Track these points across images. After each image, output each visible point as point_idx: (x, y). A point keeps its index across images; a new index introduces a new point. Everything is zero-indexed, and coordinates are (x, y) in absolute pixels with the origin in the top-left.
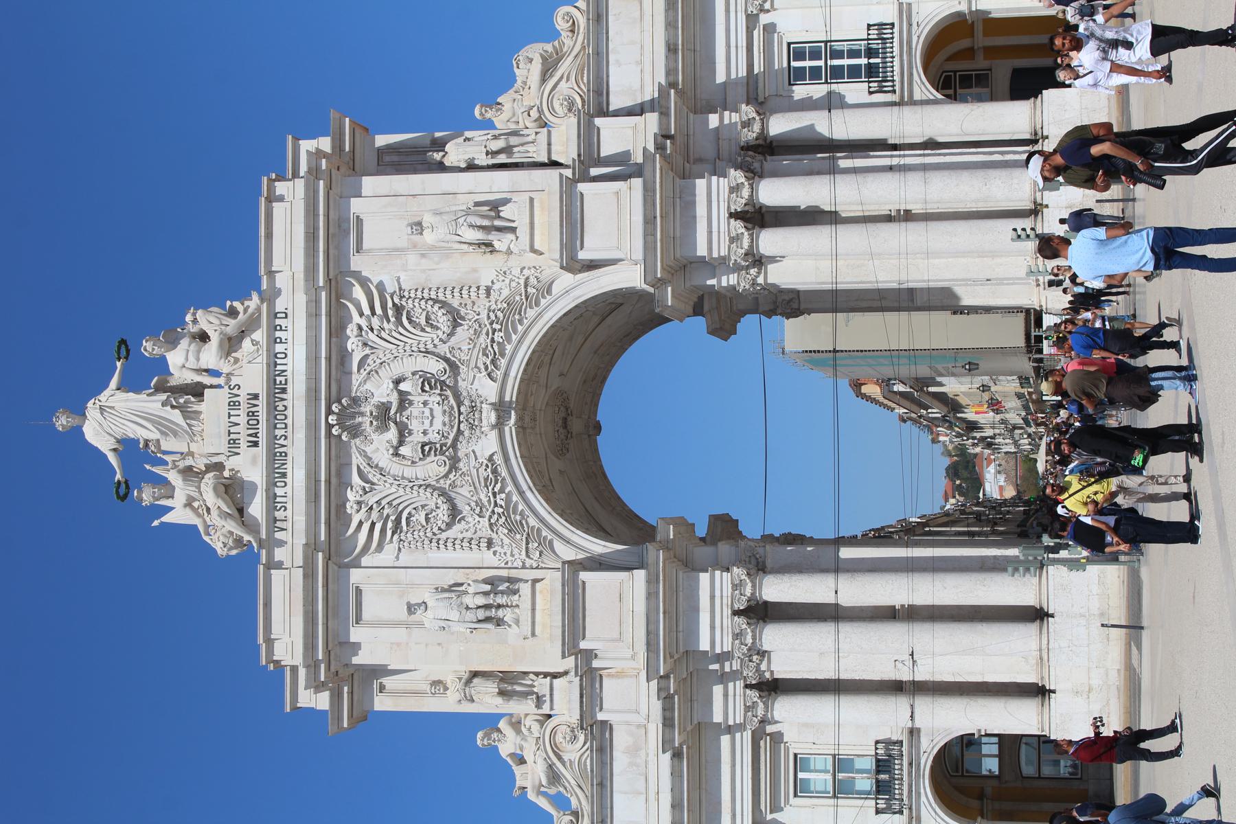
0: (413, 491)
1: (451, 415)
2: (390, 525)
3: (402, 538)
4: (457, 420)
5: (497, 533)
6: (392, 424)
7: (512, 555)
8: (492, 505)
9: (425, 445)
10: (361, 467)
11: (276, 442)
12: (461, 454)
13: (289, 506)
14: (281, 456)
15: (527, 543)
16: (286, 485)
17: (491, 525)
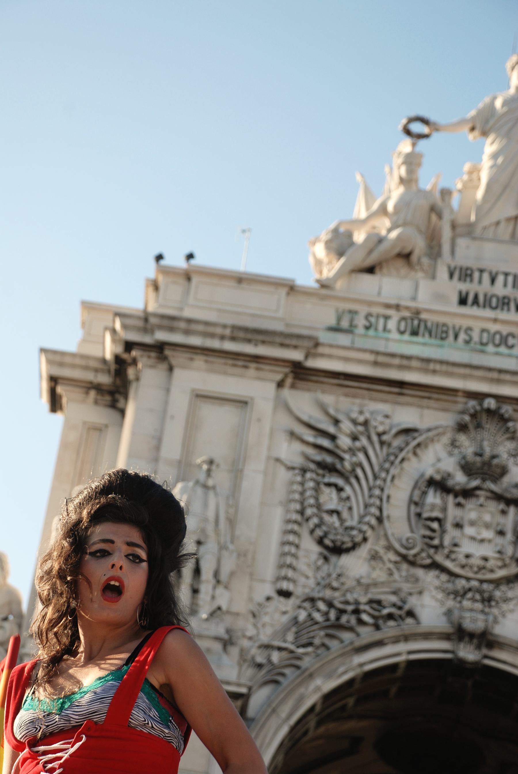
0: (372, 501)
1: (481, 568)
2: (329, 459)
3: (308, 475)
4: (470, 575)
5: (300, 607)
6: (475, 483)
7: (264, 625)
8: (341, 606)
9: (441, 525)
10: (416, 434)
11: (464, 328)
12: (420, 572)
13: (371, 332)
14: (442, 332)
15: (280, 649)
16: (402, 333)
17: (312, 600)
